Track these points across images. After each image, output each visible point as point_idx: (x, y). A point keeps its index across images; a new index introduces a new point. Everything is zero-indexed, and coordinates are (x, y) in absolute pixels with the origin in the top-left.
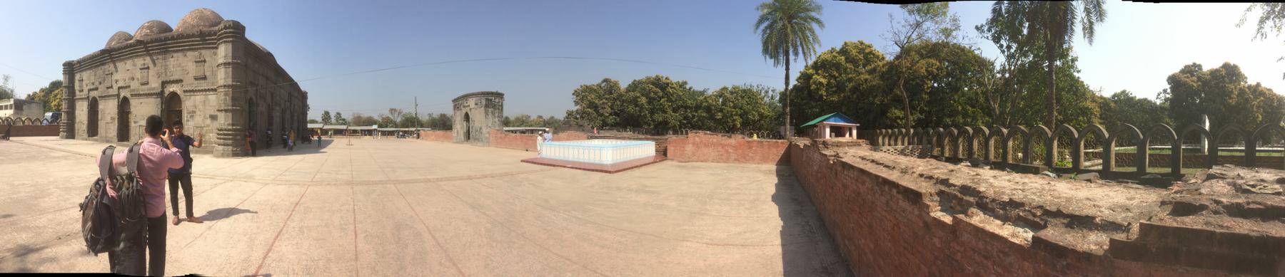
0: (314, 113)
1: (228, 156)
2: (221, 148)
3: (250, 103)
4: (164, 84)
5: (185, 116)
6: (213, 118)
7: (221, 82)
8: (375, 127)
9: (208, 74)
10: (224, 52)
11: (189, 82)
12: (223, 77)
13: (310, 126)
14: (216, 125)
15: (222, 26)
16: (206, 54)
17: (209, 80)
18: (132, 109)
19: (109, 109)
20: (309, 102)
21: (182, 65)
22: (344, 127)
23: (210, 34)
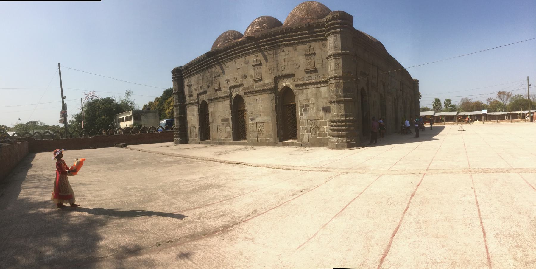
0: (426, 101)
1: (343, 147)
2: (335, 139)
3: (363, 93)
4: (277, 79)
5: (299, 110)
6: (326, 110)
7: (332, 74)
8: (484, 111)
9: (318, 66)
10: (332, 43)
11: (301, 76)
12: (332, 68)
13: (422, 114)
14: (329, 117)
15: (330, 16)
16: (316, 46)
17: (320, 72)
18: (248, 107)
19: (221, 111)
20: (421, 90)
21: (292, 58)
22: (454, 113)
23: (318, 26)
